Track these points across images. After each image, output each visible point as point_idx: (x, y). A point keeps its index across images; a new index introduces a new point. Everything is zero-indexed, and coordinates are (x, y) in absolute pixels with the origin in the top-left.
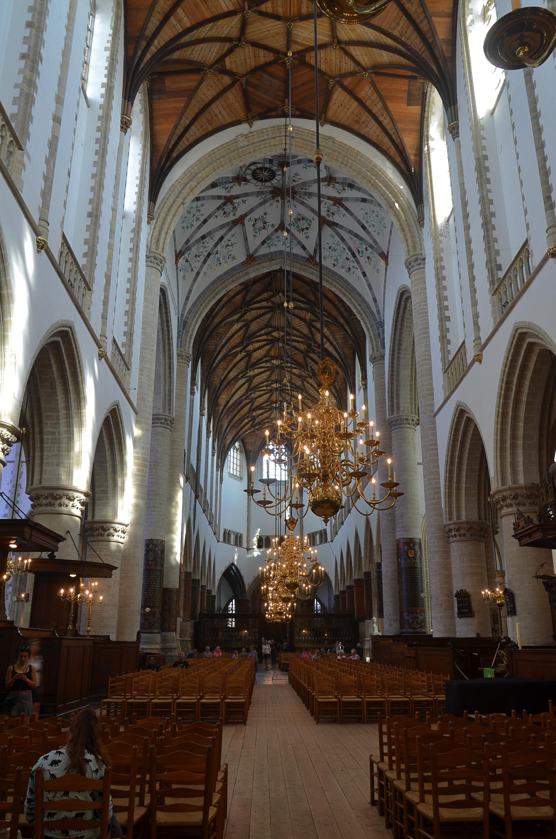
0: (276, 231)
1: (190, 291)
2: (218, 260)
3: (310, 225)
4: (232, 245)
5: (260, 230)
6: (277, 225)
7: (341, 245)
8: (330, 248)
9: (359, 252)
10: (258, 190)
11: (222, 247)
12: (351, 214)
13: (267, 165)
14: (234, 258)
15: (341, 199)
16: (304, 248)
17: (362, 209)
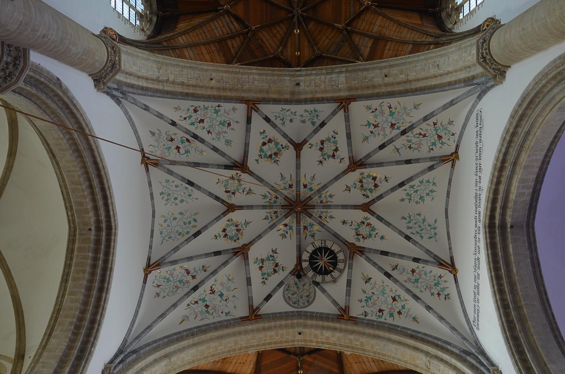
0: (305, 142)
1: (445, 107)
2: (392, 114)
3: (261, 150)
4: (369, 124)
5: (328, 140)
6: (306, 147)
7: (214, 135)
8: (229, 124)
9: (188, 140)
10: (329, 210)
11: (384, 129)
12: (210, 195)
13: (319, 278)
14: (368, 108)
15: (224, 214)
16: (267, 119)
17: (197, 199)
